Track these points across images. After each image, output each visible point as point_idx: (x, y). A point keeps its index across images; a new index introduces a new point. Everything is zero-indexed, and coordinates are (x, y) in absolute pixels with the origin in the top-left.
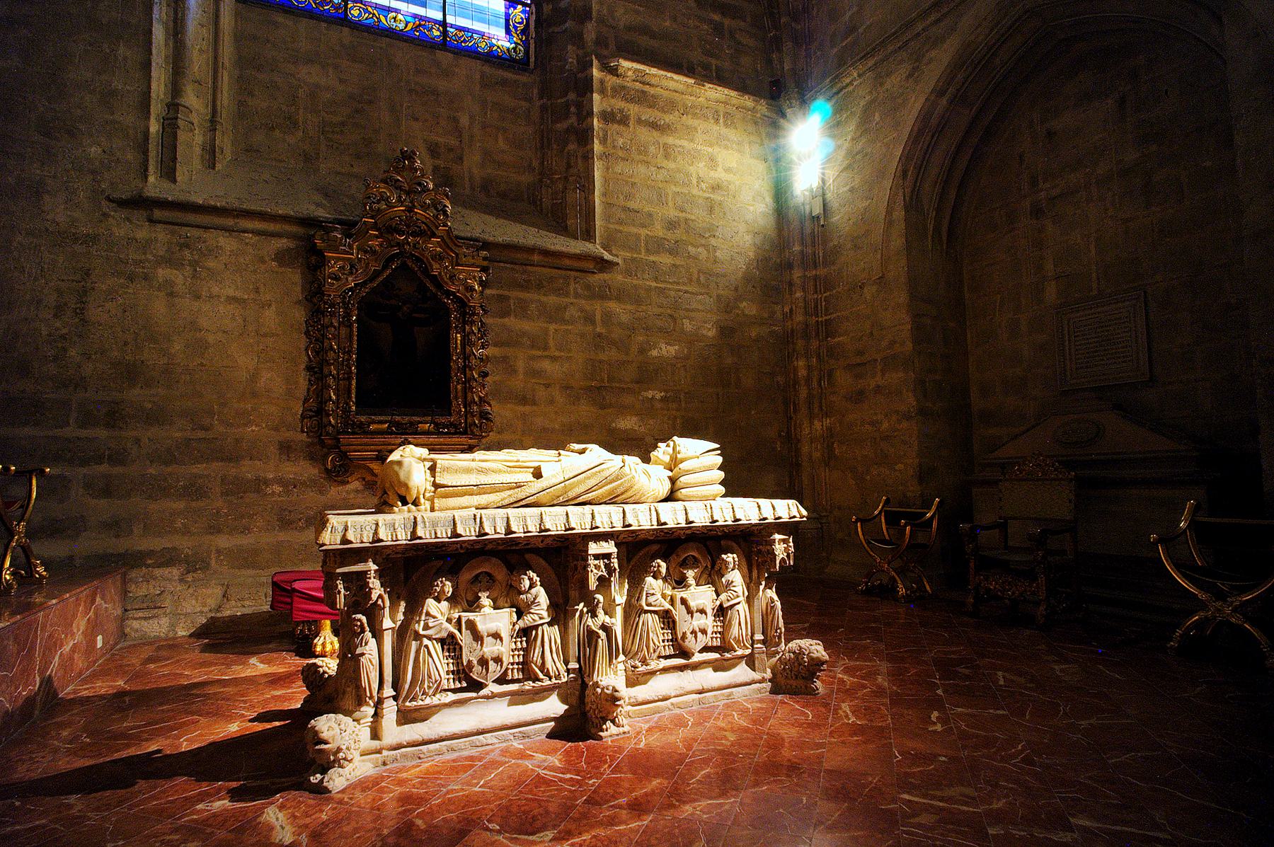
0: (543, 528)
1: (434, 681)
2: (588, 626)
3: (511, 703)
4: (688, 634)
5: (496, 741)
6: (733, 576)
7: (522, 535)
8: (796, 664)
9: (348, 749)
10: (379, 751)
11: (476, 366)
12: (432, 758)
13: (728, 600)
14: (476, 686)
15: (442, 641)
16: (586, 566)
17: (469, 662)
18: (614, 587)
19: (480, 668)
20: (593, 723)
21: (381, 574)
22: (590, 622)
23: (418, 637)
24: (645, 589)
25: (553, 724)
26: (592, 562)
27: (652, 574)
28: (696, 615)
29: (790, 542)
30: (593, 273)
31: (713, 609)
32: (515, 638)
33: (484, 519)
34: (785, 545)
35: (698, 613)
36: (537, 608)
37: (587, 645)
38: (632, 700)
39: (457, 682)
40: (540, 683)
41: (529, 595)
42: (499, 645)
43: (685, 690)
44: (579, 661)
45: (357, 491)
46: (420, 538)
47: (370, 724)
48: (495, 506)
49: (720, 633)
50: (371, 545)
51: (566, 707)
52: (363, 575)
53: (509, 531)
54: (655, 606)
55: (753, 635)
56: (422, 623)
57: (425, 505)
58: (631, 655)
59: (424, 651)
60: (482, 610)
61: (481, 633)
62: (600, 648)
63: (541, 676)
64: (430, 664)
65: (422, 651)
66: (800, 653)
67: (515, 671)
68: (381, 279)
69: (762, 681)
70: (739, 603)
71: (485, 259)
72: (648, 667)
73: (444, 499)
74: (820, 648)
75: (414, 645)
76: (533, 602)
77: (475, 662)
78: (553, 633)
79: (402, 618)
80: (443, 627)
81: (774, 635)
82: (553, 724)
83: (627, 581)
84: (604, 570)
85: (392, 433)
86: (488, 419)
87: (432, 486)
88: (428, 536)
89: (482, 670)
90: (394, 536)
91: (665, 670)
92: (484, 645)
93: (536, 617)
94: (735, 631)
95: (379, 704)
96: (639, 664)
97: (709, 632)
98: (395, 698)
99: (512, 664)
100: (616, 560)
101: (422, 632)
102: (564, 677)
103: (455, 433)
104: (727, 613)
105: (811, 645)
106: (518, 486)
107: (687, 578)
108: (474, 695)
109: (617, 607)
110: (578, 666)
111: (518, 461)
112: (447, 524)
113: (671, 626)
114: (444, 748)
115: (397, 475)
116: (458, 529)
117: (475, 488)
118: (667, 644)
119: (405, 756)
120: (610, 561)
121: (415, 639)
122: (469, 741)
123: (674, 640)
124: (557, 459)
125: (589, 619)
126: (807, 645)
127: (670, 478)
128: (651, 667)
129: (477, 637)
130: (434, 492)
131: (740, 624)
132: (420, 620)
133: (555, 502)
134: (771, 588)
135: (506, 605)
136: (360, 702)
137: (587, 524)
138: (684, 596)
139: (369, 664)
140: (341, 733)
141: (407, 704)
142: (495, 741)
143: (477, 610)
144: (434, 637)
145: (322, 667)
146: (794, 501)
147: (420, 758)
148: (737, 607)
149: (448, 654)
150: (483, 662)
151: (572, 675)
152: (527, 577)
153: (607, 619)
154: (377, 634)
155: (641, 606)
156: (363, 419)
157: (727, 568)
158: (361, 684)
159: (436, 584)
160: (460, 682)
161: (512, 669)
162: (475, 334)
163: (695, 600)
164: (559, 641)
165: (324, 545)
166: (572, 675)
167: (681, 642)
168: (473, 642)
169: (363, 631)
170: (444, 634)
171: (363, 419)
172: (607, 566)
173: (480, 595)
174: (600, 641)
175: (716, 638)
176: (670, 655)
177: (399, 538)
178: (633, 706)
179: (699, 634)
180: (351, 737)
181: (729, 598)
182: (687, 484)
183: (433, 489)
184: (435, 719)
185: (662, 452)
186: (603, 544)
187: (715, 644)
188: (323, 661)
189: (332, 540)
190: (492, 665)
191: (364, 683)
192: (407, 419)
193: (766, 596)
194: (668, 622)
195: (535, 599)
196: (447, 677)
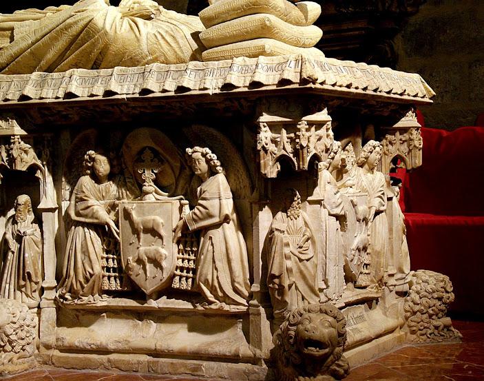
13: (195, 221)
34: (292, 135)
43: (130, 345)
54: (86, 216)
69: (254, 360)
83: (63, 180)
96: (68, 296)
107: (144, 181)
118: (114, 274)
148: (212, 233)
174: (10, 254)
178: (61, 351)
179: (149, 266)
181: (194, 216)
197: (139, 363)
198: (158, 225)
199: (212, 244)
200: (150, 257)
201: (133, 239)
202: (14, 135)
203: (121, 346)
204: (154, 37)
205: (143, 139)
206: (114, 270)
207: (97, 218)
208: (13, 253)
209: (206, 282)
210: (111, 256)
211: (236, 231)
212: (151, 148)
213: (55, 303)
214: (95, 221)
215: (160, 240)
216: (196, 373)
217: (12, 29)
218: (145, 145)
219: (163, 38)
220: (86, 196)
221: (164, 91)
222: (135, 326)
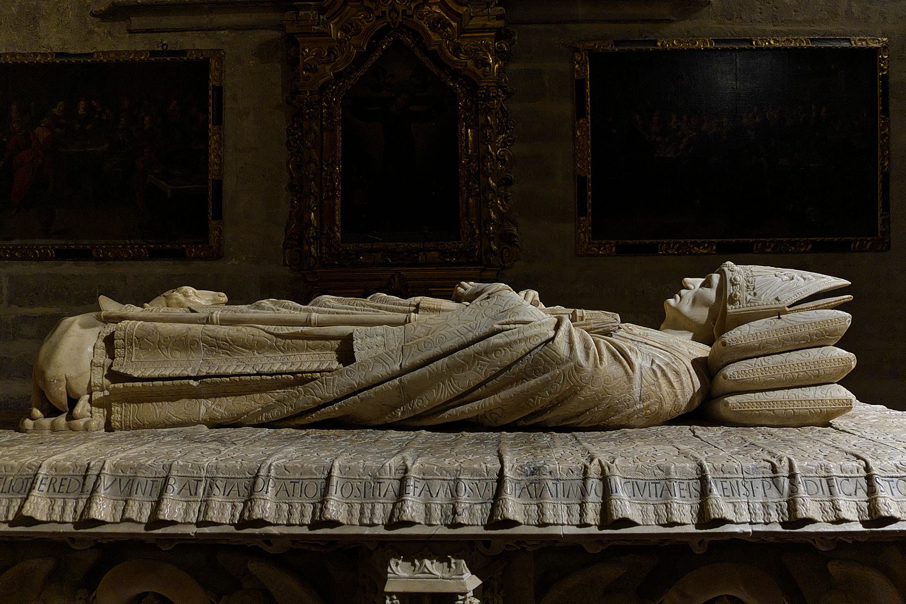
11: (493, 171)
30: (669, 21)
68: (369, 64)
71: (499, 17)
106: (300, 379)
111: (308, 323)
133: (388, 419)
137: (379, 508)
162: (492, 128)
182: (743, 382)
202: (464, 594)
204: (650, 373)
212: (727, 596)
217: (347, 341)
219: (665, 374)
221: (840, 521)
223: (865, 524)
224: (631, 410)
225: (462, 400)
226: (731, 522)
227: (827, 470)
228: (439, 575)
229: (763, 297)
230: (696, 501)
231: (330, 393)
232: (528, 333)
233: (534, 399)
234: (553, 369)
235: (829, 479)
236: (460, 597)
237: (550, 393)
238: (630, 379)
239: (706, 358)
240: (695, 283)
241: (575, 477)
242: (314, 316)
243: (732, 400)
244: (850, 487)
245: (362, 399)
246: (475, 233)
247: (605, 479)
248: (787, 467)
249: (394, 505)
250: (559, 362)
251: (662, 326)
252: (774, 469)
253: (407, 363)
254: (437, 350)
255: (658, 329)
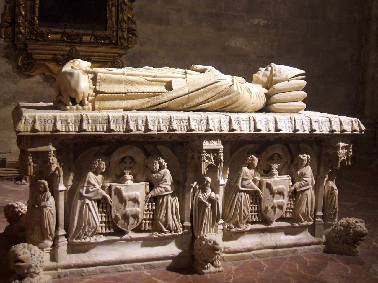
0: (171, 128)
1: (92, 227)
2: (199, 198)
3: (143, 246)
4: (270, 208)
5: (132, 269)
6: (306, 170)
7: (156, 133)
8: (345, 234)
9: (36, 266)
10: (56, 269)
12: (90, 276)
13: (300, 187)
14: (120, 232)
15: (98, 202)
16: (200, 157)
17: (116, 217)
18: (220, 173)
19: (123, 221)
20: (198, 263)
21: (57, 154)
22: (200, 195)
23: (82, 197)
24: (242, 175)
25: (171, 261)
26: (205, 154)
27: (247, 165)
28: (277, 196)
29: (350, 149)
31: (289, 192)
32: (148, 203)
33: (130, 120)
34: (347, 151)
35: (278, 195)
36: (164, 184)
37: (197, 211)
38: (226, 250)
39: (107, 229)
40: (164, 234)
41: (159, 174)
42: (136, 207)
44: (191, 221)
45: (39, 83)
46: (85, 131)
47: (50, 251)
48: (138, 109)
49: (292, 209)
50: (51, 134)
51: (180, 251)
52: (46, 154)
53: (147, 129)
54: (248, 188)
55: (316, 211)
56: (85, 188)
57: (89, 105)
58: (228, 219)
59: (86, 207)
60: (126, 182)
61: (125, 198)
62: (206, 215)
63: (165, 230)
64: (90, 216)
65: (84, 207)
66: (347, 227)
67: (147, 225)
70: (308, 189)
72: (240, 229)
73: (102, 102)
74: (363, 225)
75: (79, 203)
76: (161, 180)
77: (120, 217)
78: (176, 201)
79: (71, 184)
80: (99, 192)
81: (331, 213)
82: (171, 261)
84: (213, 161)
85: (64, 41)
86: (133, 34)
87: (93, 86)
88: (90, 130)
89: (125, 222)
90: (67, 128)
91: (251, 232)
92: (127, 206)
93: (163, 190)
94: (303, 208)
95: (56, 239)
96: (233, 226)
97: (285, 207)
98: (66, 236)
99: (145, 220)
100: (222, 154)
101: (84, 194)
102: (180, 231)
103: (110, 44)
104: (300, 195)
105: (357, 222)
107: (273, 169)
108: (118, 238)
109: (220, 187)
110: (190, 225)
111: (155, 76)
112: (104, 122)
113: (258, 201)
114: (98, 271)
115: (69, 83)
116: (111, 126)
117: (124, 95)
118: (254, 214)
119: (72, 273)
120: (218, 154)
121: (80, 199)
122: (114, 267)
123: (259, 211)
124: (184, 76)
125: (200, 194)
126: (354, 222)
127: (266, 94)
128: (242, 229)
129: (122, 200)
130: (95, 96)
131: (307, 204)
132: (83, 187)
133: (181, 108)
134: (332, 180)
135: (143, 180)
136: (44, 237)
137: (203, 127)
138: (269, 182)
139: (50, 213)
140: (31, 257)
141: (75, 241)
142: (132, 269)
143: (123, 182)
144: (93, 198)
145: (17, 208)
146: (357, 119)
147: (82, 275)
148: (307, 192)
149: (101, 210)
150: (126, 217)
151: (185, 230)
152: (158, 162)
153: (213, 195)
154: (55, 193)
155: (238, 187)
156: (44, 30)
157: (302, 164)
158: (44, 226)
159: (95, 162)
160: (109, 229)
161: (145, 223)
163: (276, 185)
164: (178, 206)
165: (19, 132)
166: (185, 230)
167: (264, 214)
168: (119, 203)
169: (45, 191)
170: (99, 197)
171: (44, 30)
172: (215, 158)
173: (125, 172)
174: (207, 209)
175: (289, 212)
176: (255, 221)
177: (71, 130)
178: (227, 253)
179: (277, 209)
180: (38, 259)
181: (301, 186)
183: (94, 94)
184: (93, 251)
185: (262, 73)
186: (214, 142)
187: (288, 216)
188: (18, 204)
189: (26, 128)
190: (131, 220)
191: (46, 225)
192: (76, 31)
193: (328, 186)
194: (256, 199)
195: (163, 177)
196: (101, 225)
197: (269, 253)
198: (284, 190)
199: (307, 197)
200: (279, 204)
201: (270, 197)
202: (221, 149)
203: (259, 247)
205: (278, 149)
206: (255, 212)
207: (253, 188)
208: (208, 209)
209: (302, 214)
210: (254, 205)
211: (313, 190)
213: (223, 231)
214: (252, 189)
215: (283, 197)
216: (294, 253)
218: (276, 152)
219: (259, 97)
220: (249, 178)
221: (305, 131)
222: (261, 236)
223: (309, 131)
224: (250, 106)
225: (204, 102)
226: (282, 131)
227: (302, 119)
228: (216, 144)
229: (283, 75)
230: (274, 126)
231: (165, 99)
232: (226, 83)
233: (226, 102)
234: (232, 93)
235: (302, 122)
236: (221, 150)
237: (231, 100)
238: (251, 97)
239: (267, 93)
240: (263, 69)
241: (247, 120)
242: (158, 75)
243: (275, 105)
244: (306, 123)
245: (175, 101)
246: (114, 28)
247: (254, 120)
248: (294, 119)
249: (206, 126)
250: (234, 92)
251: (252, 82)
252: (291, 119)
253: (190, 90)
254: (200, 87)
255: (251, 83)
